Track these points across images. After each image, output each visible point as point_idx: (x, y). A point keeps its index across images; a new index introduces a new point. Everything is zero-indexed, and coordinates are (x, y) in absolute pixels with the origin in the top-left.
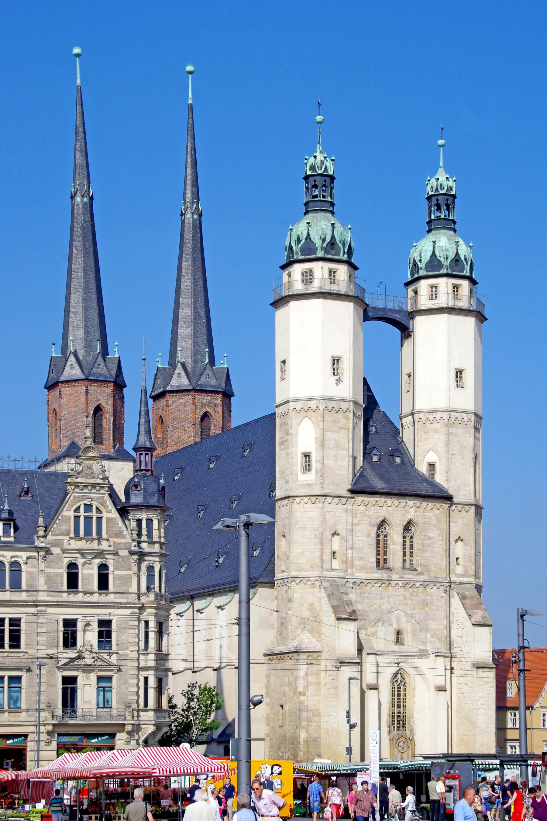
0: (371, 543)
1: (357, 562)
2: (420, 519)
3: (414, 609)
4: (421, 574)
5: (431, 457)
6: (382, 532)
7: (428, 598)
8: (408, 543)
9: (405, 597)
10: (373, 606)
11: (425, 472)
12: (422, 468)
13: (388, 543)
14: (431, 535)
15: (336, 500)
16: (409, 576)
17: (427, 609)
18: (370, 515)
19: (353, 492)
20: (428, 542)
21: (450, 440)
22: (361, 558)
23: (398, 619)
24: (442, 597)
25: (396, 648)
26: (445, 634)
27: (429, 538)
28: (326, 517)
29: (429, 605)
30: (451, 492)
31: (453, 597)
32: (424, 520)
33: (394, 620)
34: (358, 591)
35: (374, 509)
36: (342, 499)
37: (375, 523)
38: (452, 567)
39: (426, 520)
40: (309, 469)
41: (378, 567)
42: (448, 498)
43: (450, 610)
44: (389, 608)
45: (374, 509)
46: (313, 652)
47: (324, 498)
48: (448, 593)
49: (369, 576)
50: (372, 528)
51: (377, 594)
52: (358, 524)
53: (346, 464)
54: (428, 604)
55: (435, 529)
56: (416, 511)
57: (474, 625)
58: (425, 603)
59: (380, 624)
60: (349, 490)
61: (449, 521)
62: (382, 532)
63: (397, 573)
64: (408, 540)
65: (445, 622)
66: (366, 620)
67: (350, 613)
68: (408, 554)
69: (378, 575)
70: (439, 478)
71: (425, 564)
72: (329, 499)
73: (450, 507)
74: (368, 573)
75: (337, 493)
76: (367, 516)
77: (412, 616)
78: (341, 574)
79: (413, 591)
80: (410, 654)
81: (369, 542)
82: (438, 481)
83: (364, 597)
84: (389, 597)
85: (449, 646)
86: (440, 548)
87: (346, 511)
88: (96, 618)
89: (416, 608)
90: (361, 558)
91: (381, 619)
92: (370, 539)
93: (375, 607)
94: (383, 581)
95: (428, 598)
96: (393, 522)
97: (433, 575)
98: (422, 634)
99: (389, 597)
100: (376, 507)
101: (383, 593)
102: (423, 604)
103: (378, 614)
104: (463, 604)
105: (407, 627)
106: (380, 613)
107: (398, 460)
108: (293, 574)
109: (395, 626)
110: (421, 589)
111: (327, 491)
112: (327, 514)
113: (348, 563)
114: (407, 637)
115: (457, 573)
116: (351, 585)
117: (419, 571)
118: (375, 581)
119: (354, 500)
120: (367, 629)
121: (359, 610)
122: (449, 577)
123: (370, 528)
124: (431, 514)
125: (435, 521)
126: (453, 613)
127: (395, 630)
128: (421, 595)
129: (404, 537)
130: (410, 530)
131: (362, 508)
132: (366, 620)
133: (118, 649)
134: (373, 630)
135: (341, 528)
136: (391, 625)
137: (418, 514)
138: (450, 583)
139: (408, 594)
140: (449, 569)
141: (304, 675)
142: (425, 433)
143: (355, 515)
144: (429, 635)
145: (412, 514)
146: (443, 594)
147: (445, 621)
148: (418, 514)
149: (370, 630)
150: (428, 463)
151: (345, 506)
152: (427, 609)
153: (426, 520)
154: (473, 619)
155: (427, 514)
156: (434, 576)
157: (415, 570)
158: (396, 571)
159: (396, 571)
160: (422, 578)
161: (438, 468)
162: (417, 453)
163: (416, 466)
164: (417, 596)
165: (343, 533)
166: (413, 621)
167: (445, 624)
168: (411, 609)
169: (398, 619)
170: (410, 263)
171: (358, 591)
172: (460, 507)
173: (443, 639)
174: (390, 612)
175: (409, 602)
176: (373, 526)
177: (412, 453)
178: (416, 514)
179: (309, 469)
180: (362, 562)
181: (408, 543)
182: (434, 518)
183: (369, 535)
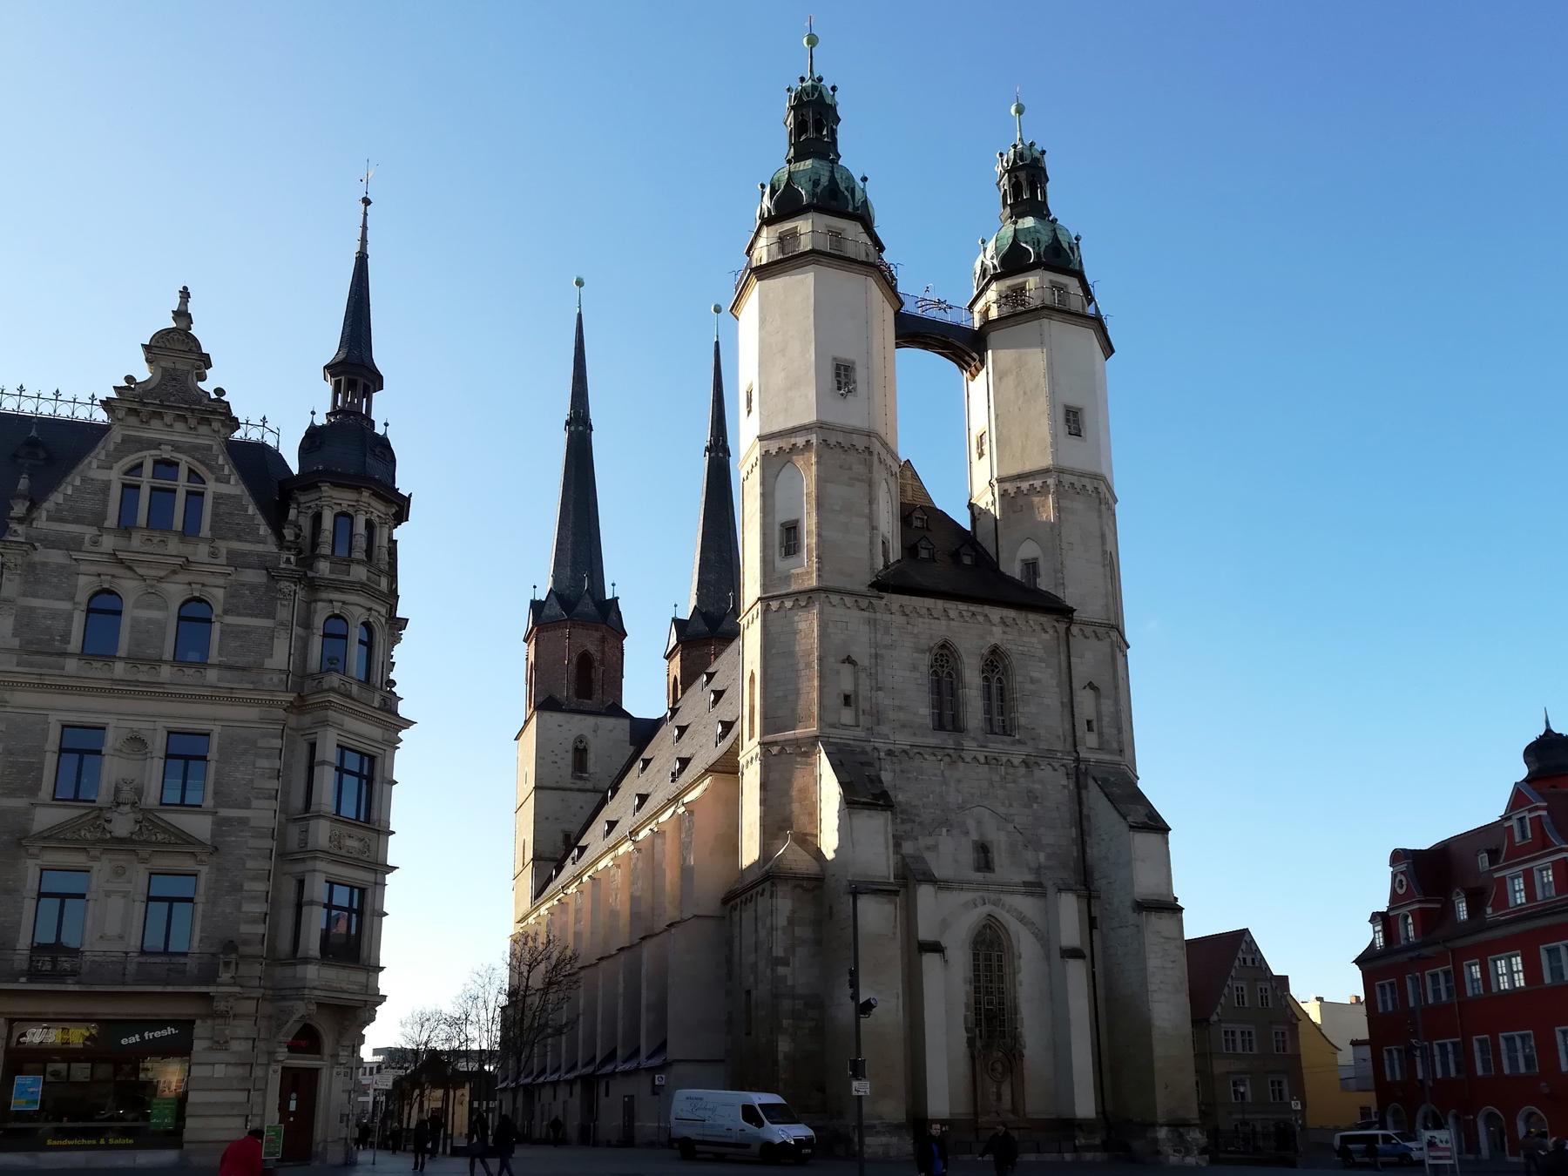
0: (920, 681)
1: (892, 715)
2: (1014, 647)
3: (1011, 805)
4: (1020, 742)
5: (1029, 550)
6: (943, 666)
7: (1037, 786)
8: (994, 691)
9: (991, 783)
10: (928, 797)
11: (1018, 577)
12: (1013, 569)
13: (955, 687)
14: (1036, 675)
15: (849, 601)
16: (997, 746)
17: (1035, 806)
18: (915, 632)
19: (883, 585)
20: (1029, 686)
21: (1062, 518)
22: (900, 708)
23: (979, 822)
24: (1064, 786)
25: (979, 876)
26: (1075, 854)
27: (1033, 681)
28: (829, 630)
29: (1039, 800)
30: (1069, 603)
31: (1086, 787)
32: (1020, 648)
33: (971, 824)
34: (898, 768)
35: (924, 623)
36: (859, 600)
37: (926, 648)
38: (1079, 734)
39: (1026, 649)
40: (795, 550)
41: (940, 726)
42: (1060, 611)
43: (1081, 812)
44: (960, 801)
45: (924, 623)
46: (803, 879)
47: (823, 595)
48: (1074, 779)
49: (919, 740)
50: (921, 656)
51: (935, 775)
52: (891, 646)
53: (867, 541)
54: (1037, 797)
55: (1043, 665)
56: (1004, 632)
57: (1131, 827)
58: (1032, 797)
59: (944, 830)
60: (873, 585)
61: (1069, 651)
62: (943, 666)
63: (973, 739)
64: (995, 685)
65: (1074, 832)
66: (914, 822)
67: (873, 794)
68: (995, 711)
69: (934, 739)
70: (1044, 584)
71: (1029, 727)
72: (835, 599)
73: (1068, 629)
74: (915, 734)
75: (849, 587)
76: (911, 633)
77: (1007, 819)
78: (860, 733)
79: (1007, 774)
80: (1005, 888)
81: (916, 679)
82: (1044, 589)
83: (909, 778)
84: (959, 781)
85: (1082, 878)
86: (1052, 699)
87: (873, 623)
88: (162, 726)
89: (1015, 804)
90: (900, 708)
91: (945, 822)
92: (918, 675)
93: (931, 796)
94: (947, 750)
95: (1037, 786)
96: (961, 650)
97: (1043, 746)
98: (1029, 853)
99: (959, 781)
100: (926, 620)
101: (947, 773)
102: (1028, 796)
103: (938, 812)
104: (1106, 795)
105: (999, 840)
106: (943, 811)
107: (967, 560)
108: (770, 738)
109: (975, 836)
110: (1023, 770)
111: (830, 584)
112: (831, 624)
113: (877, 715)
114: (1000, 858)
115: (1088, 745)
116: (882, 755)
117: (1017, 737)
118: (931, 750)
119: (884, 601)
120: (917, 840)
121: (899, 803)
122: (1076, 751)
123: (915, 655)
124: (1035, 640)
125: (1042, 651)
126: (1088, 816)
127: (975, 842)
128: (1022, 780)
129: (986, 679)
130: (997, 667)
131: (899, 619)
132: (914, 822)
133: (217, 805)
134: (930, 841)
135: (861, 654)
136: (967, 833)
137: (1010, 637)
138: (1078, 760)
139: (997, 778)
140: (1075, 736)
141: (785, 923)
142: (1014, 512)
143: (887, 631)
144: (1042, 857)
145: (997, 636)
146: (1065, 782)
147: (1074, 830)
148: (1010, 637)
149: (924, 841)
150: (1022, 561)
151: (866, 614)
152: (1035, 806)
153: (1026, 649)
154: (1130, 819)
155: (1025, 639)
156: (1046, 748)
157: (1010, 735)
158: (972, 735)
159: (972, 735)
160: (1024, 750)
161: (1043, 567)
162: (1002, 546)
163: (1002, 569)
164: (1014, 782)
165: (864, 660)
166: (1010, 827)
167: (1074, 836)
168: (1003, 805)
169: (979, 822)
170: (975, 273)
171: (898, 768)
172: (1088, 630)
173: (1072, 864)
174: (961, 808)
175: (1000, 793)
176: (923, 652)
177: (992, 552)
178: (1006, 637)
179: (795, 550)
180: (902, 716)
181: (994, 691)
182: (1040, 646)
183: (915, 668)
